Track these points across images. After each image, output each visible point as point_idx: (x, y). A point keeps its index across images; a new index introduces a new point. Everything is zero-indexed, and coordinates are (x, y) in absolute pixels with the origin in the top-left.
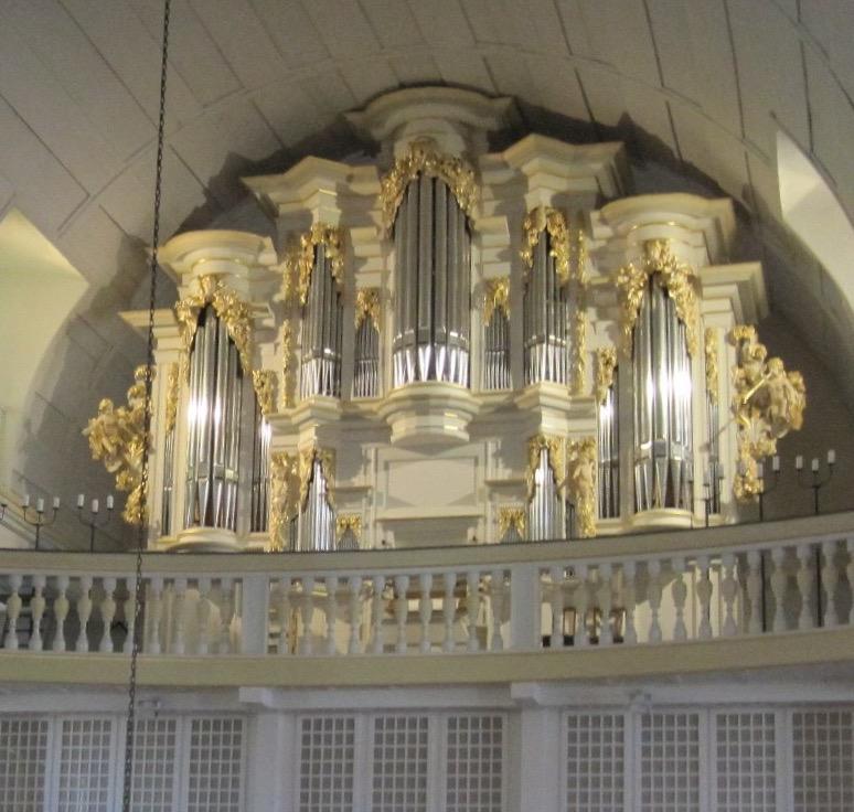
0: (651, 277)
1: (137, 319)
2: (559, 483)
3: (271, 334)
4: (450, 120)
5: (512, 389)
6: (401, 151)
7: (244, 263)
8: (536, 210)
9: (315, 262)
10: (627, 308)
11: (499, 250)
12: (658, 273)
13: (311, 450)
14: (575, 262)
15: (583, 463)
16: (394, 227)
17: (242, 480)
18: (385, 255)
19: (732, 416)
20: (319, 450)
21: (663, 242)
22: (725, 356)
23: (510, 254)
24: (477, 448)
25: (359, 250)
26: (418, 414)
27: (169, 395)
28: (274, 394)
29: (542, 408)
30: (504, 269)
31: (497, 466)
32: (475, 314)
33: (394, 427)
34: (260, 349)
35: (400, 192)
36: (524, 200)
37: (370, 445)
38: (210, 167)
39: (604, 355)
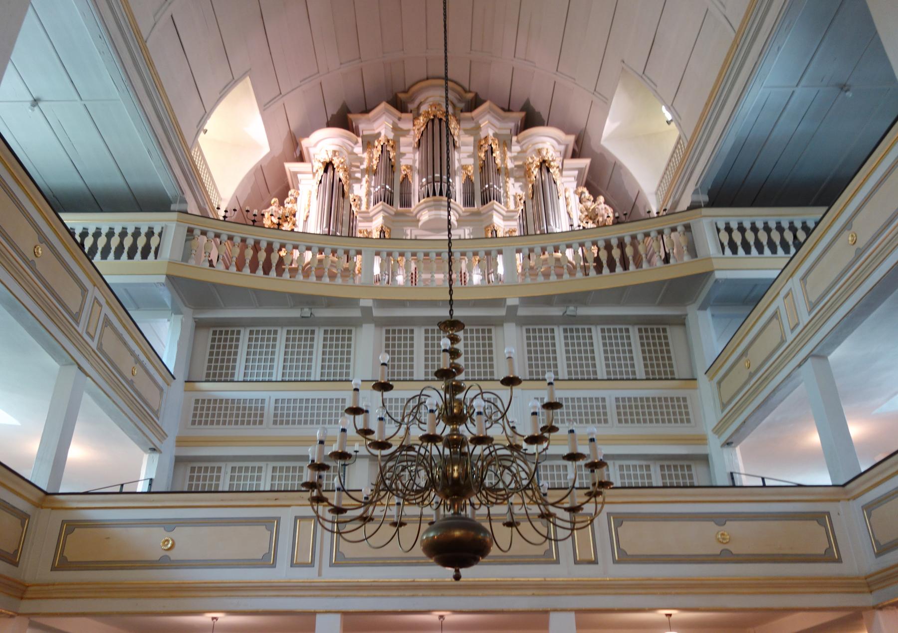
0: (541, 164)
3: (359, 181)
6: (424, 108)
7: (347, 150)
10: (529, 177)
12: (544, 161)
14: (503, 160)
18: (414, 153)
22: (574, 200)
23: (473, 155)
26: (436, 209)
27: (307, 203)
28: (360, 205)
30: (471, 161)
32: (457, 179)
38: (333, 110)
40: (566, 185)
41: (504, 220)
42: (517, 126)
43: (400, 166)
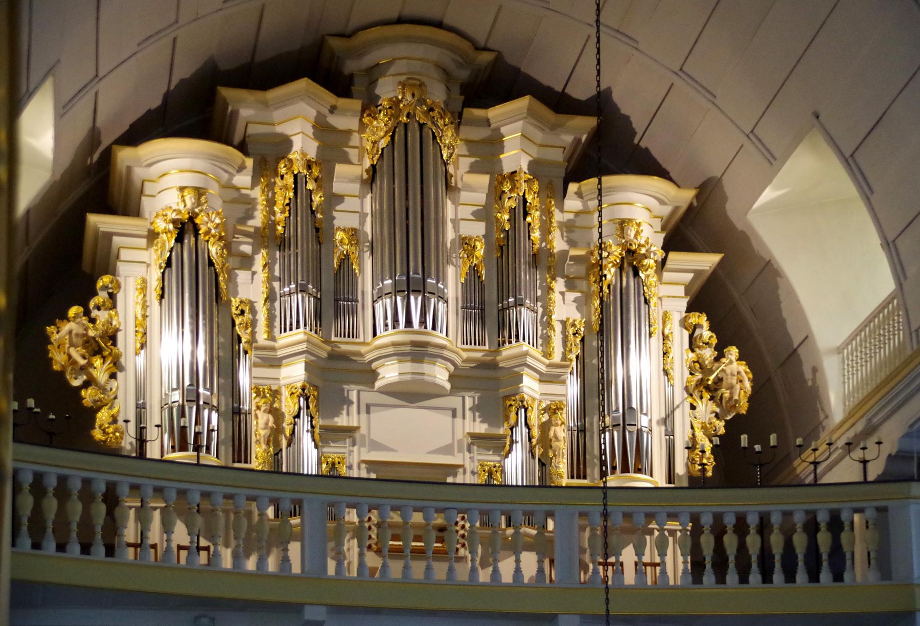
1: (98, 221)
2: (534, 441)
4: (438, 66)
5: (487, 347)
6: (387, 89)
8: (515, 172)
9: (296, 193)
11: (475, 208)
13: (299, 385)
14: (546, 231)
15: (557, 425)
16: (373, 166)
17: (222, 408)
18: (362, 197)
19: (686, 395)
20: (308, 386)
21: (639, 225)
22: (679, 338)
23: (484, 214)
24: (455, 401)
25: (338, 187)
28: (254, 323)
29: (526, 370)
31: (474, 420)
32: (451, 271)
33: (379, 371)
34: (237, 275)
35: (386, 133)
36: (500, 161)
37: (353, 386)
38: (184, 70)
39: (573, 325)
40: (668, 305)
41: (541, 381)
42: (577, 141)
43: (332, 231)
